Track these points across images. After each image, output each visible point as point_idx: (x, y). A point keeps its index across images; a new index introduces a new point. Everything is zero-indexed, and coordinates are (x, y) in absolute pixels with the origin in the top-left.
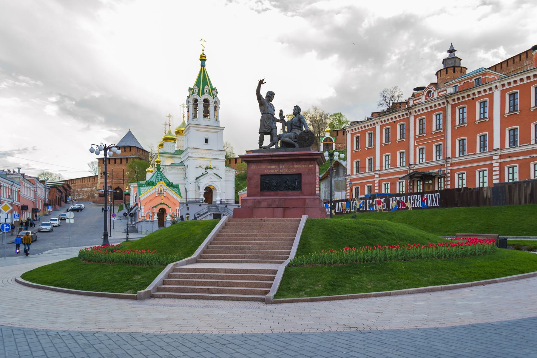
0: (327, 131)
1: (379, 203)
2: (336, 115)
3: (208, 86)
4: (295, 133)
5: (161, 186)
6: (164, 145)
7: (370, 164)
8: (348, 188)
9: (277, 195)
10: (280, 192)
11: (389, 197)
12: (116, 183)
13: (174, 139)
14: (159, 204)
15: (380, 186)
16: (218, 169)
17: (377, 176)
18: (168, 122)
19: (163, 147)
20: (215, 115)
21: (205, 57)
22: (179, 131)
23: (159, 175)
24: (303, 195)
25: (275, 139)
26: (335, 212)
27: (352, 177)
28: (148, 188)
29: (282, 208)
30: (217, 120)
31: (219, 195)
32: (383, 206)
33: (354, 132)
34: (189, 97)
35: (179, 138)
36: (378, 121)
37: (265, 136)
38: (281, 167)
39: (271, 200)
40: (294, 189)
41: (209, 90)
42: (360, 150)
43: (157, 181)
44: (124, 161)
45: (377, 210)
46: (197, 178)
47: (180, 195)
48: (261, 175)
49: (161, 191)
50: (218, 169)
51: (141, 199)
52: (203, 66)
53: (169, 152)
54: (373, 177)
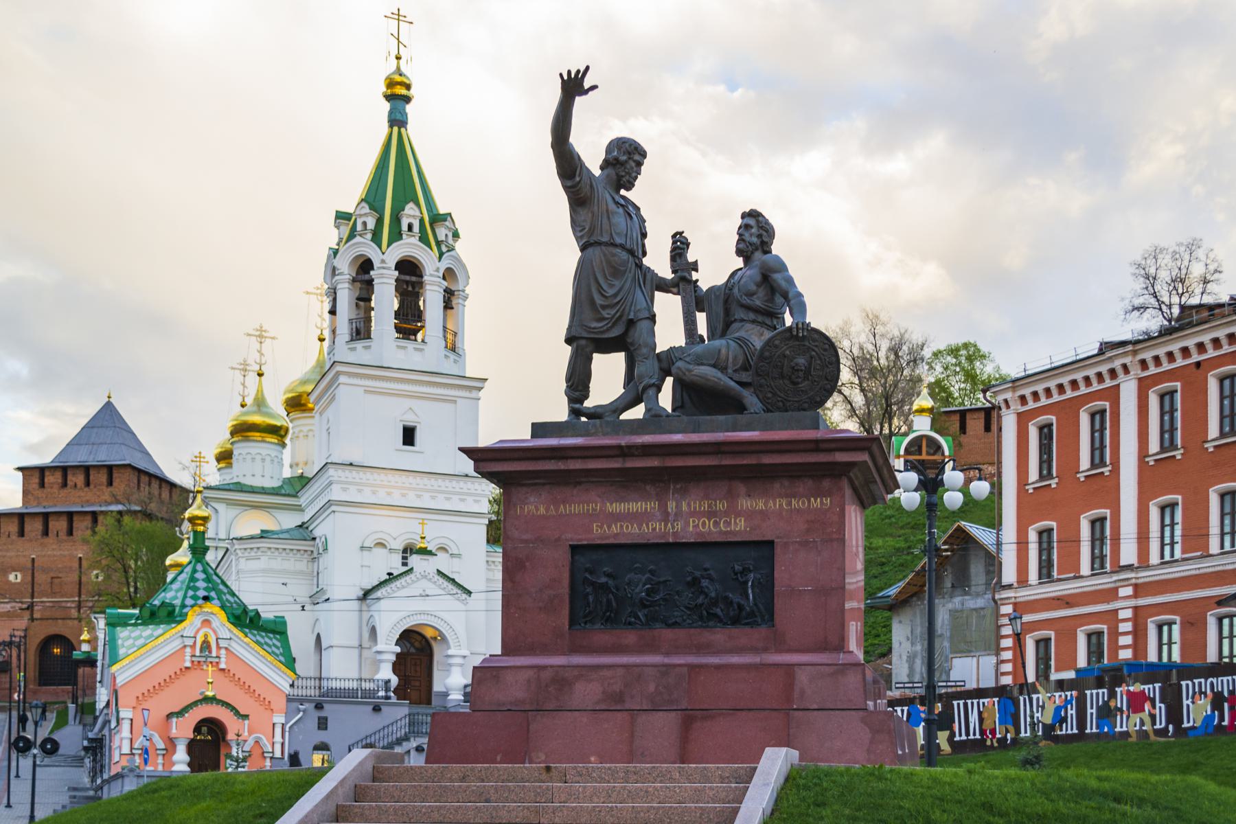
0: (921, 411)
1: (1136, 703)
2: (958, 350)
3: (418, 205)
4: (742, 342)
5: (206, 622)
6: (235, 453)
7: (1097, 539)
8: (1007, 643)
9: (651, 648)
10: (668, 634)
11: (1180, 678)
12: (48, 614)
13: (277, 432)
14: (195, 704)
15: (1139, 633)
16: (458, 556)
17: (1129, 591)
18: (253, 358)
19: (230, 465)
20: (445, 327)
21: (408, 87)
22: (299, 396)
23: (200, 575)
24: (781, 645)
25: (646, 368)
26: (951, 740)
27: (1024, 594)
28: (148, 631)
29: (673, 714)
30: (453, 349)
31: (461, 665)
32: (1153, 717)
33: (1031, 405)
34: (336, 252)
35: (296, 425)
36: (1127, 360)
37: (595, 355)
38: (671, 506)
39: (620, 672)
40: (739, 617)
41: (422, 221)
42: (1053, 483)
43: (189, 602)
44: (82, 525)
45: (1126, 735)
46: (366, 594)
47: (290, 662)
48: (575, 549)
49: (206, 645)
50: (458, 556)
51: (120, 681)
52: (397, 121)
53: (257, 482)
54: (1111, 594)
